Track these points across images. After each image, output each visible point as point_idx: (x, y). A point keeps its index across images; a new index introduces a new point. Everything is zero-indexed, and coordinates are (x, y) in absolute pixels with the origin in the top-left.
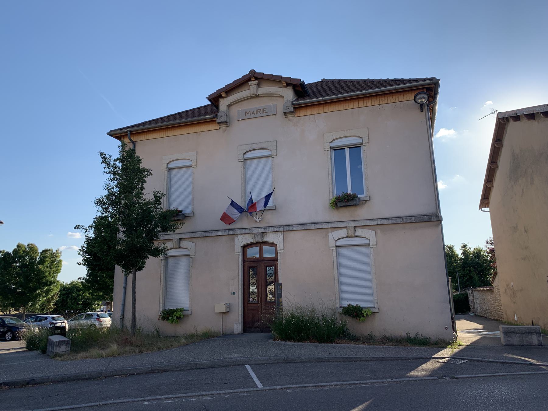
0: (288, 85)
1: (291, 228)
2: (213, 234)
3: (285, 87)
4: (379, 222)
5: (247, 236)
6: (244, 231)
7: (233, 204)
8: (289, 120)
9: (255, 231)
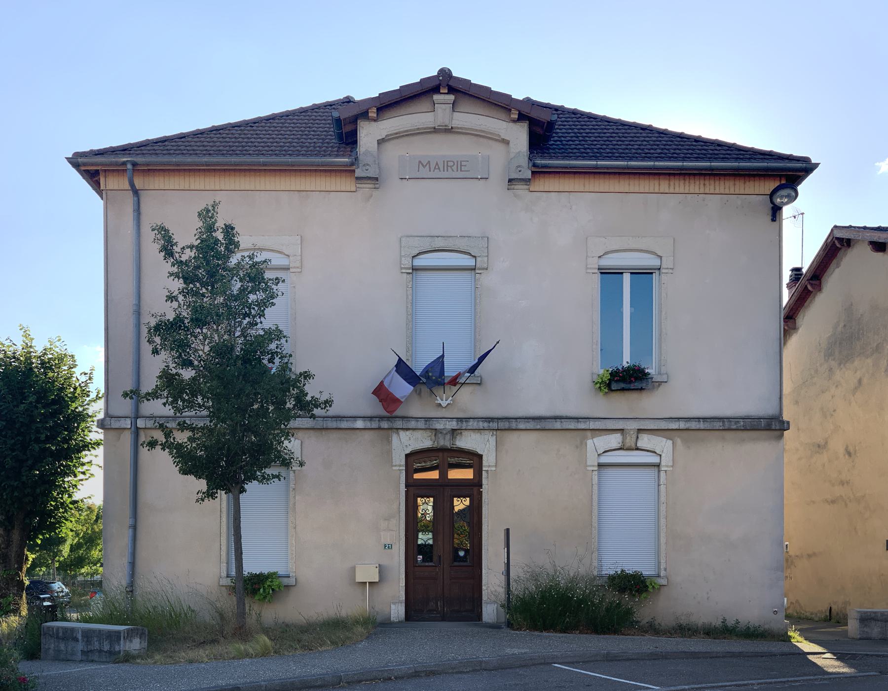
0: (522, 117)
1: (514, 425)
2: (344, 424)
3: (514, 121)
4: (682, 425)
5: (418, 434)
6: (413, 424)
7: (402, 368)
8: (515, 196)
9: (439, 426)
